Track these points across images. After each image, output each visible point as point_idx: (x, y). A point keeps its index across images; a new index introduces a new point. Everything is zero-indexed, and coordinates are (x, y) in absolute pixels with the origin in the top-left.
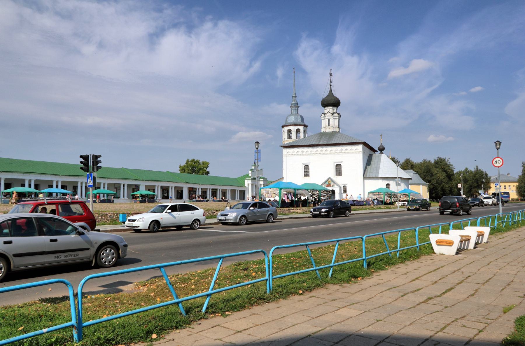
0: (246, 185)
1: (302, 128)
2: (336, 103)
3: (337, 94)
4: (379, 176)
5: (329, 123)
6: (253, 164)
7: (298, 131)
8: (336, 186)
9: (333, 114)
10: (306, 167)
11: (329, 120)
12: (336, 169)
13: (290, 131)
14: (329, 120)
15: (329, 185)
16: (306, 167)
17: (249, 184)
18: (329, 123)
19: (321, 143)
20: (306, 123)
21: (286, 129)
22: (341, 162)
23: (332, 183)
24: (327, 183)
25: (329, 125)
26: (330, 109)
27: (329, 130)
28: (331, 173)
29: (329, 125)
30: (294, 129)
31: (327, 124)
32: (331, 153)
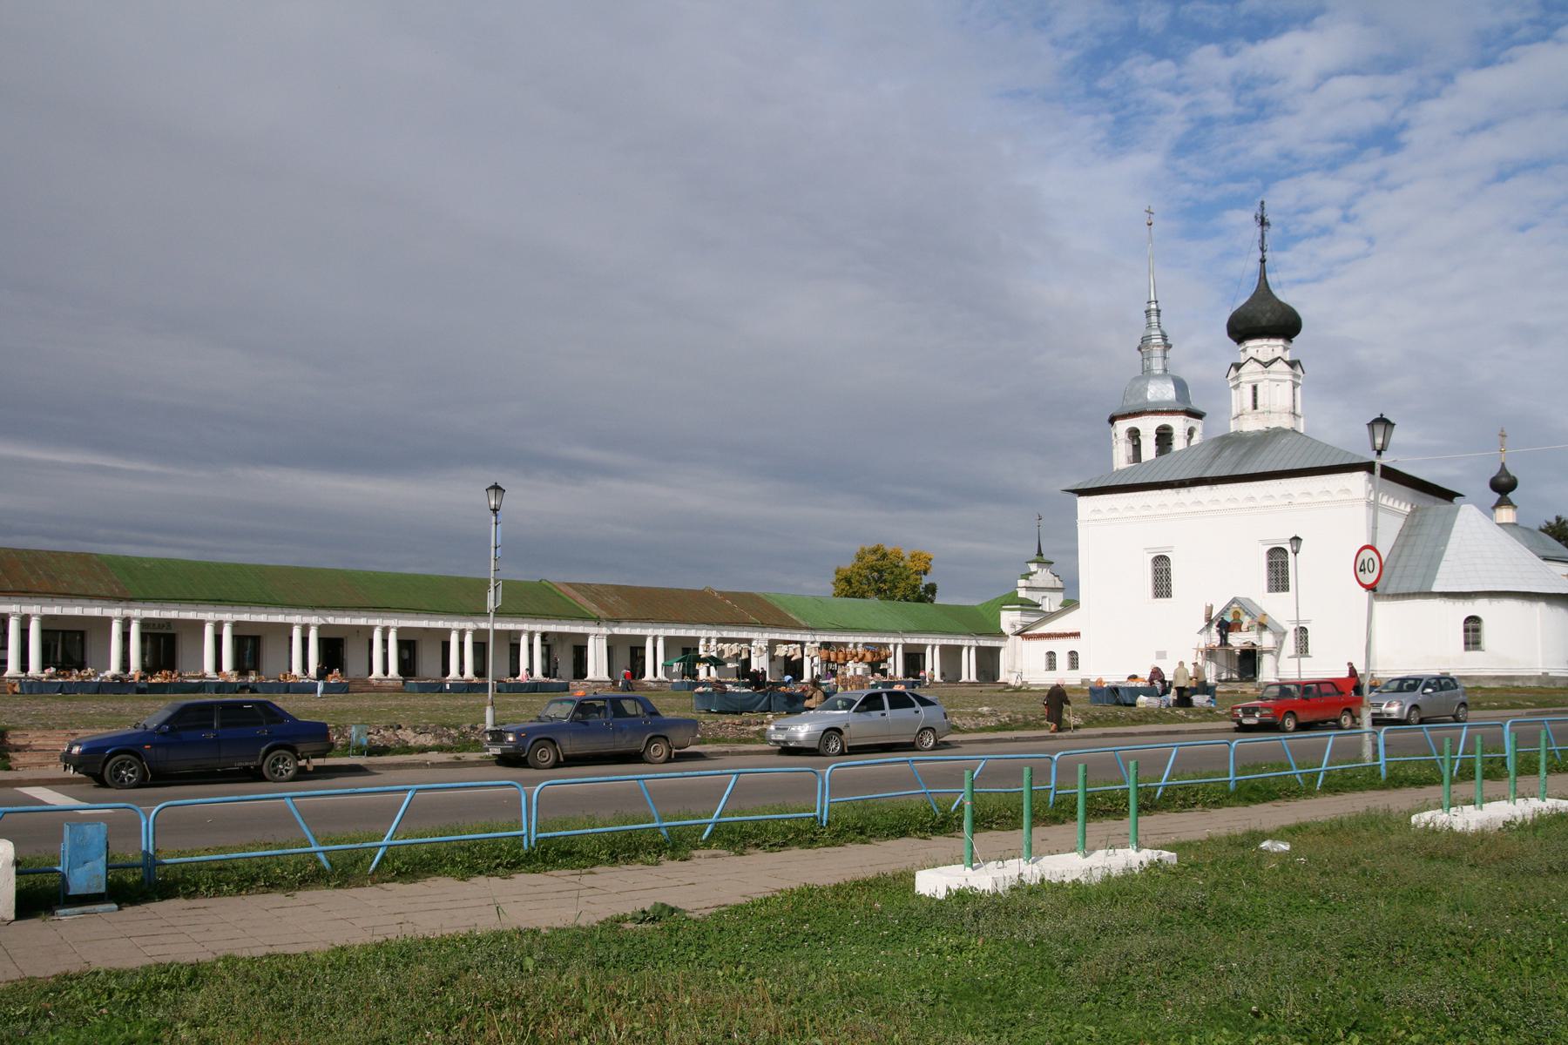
0: (1005, 627)
1: (1178, 424)
2: (1286, 326)
4: (1435, 589)
5: (1255, 401)
6: (1035, 557)
9: (1266, 365)
10: (1161, 566)
11: (1255, 388)
12: (1270, 565)
13: (1134, 434)
14: (1255, 388)
16: (1161, 566)
18: (1255, 401)
19: (1208, 474)
20: (1196, 405)
21: (1122, 426)
25: (1255, 407)
27: (1251, 425)
28: (1252, 585)
29: (1255, 407)
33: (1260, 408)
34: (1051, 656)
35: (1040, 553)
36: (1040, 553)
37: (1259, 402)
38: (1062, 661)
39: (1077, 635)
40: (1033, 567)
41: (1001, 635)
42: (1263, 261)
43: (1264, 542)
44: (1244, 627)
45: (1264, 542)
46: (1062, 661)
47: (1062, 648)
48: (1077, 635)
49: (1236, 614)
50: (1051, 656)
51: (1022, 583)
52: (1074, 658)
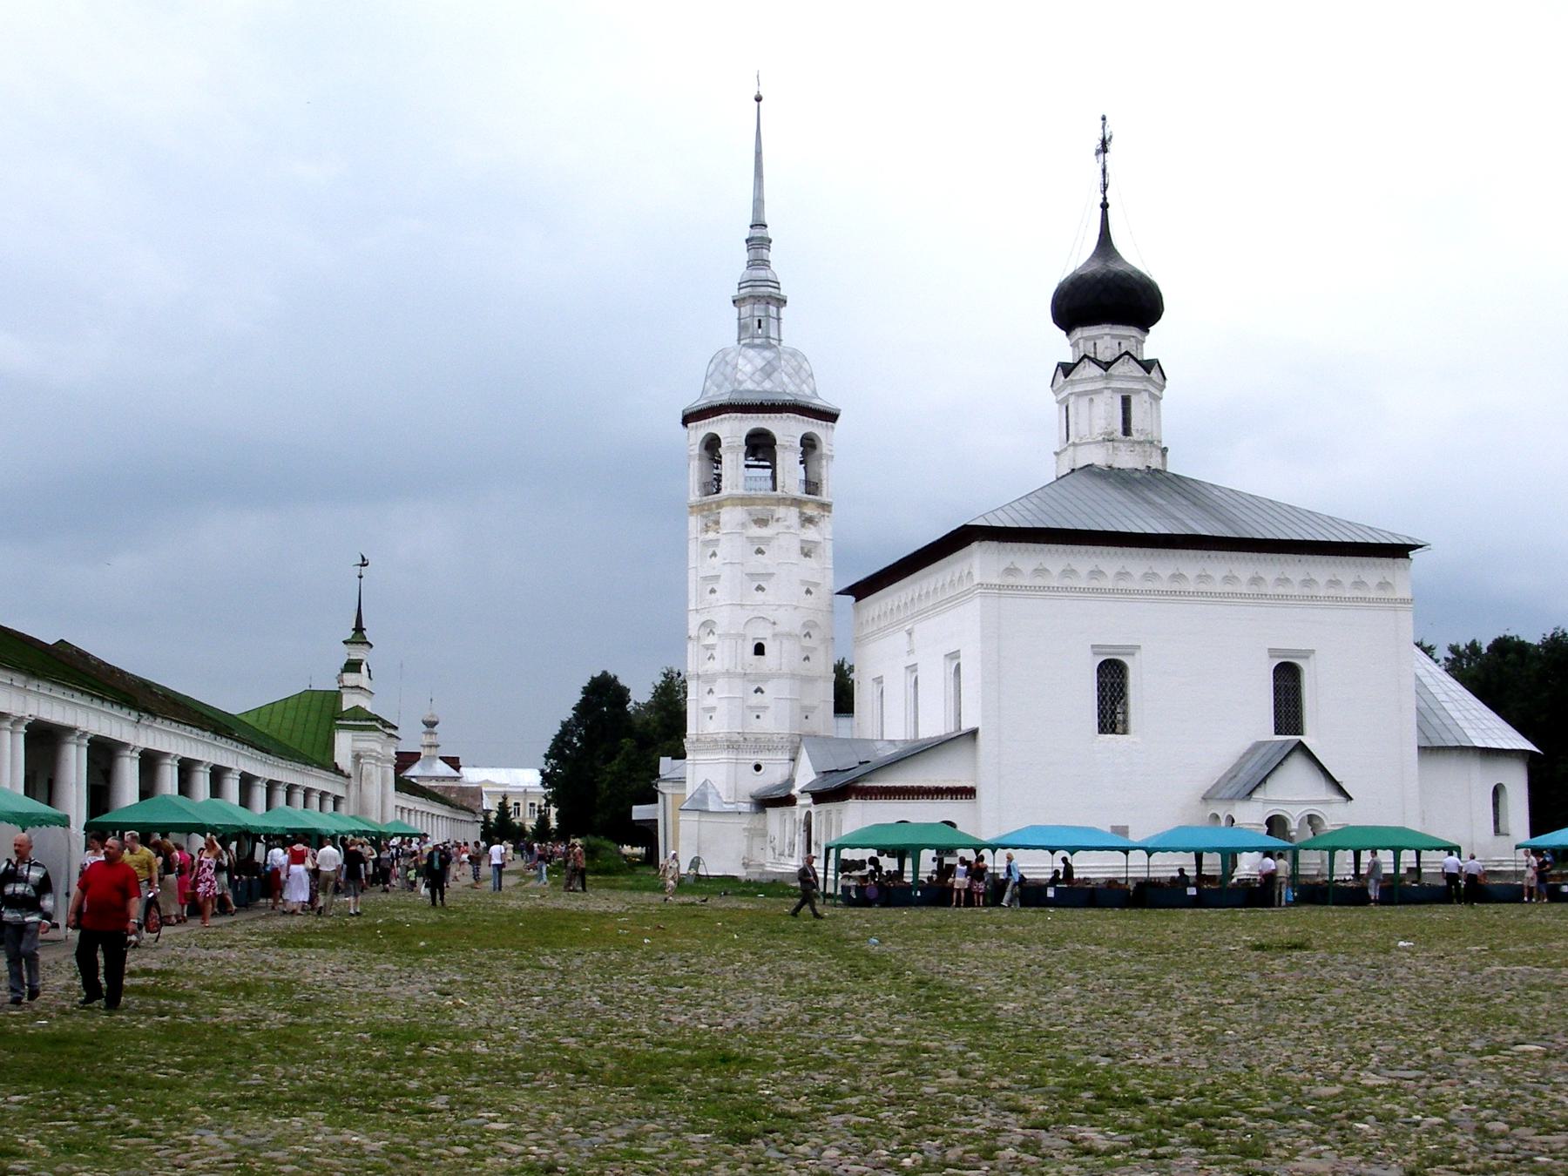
0: (343, 757)
3: (1138, 253)
6: (349, 635)
10: (1112, 679)
11: (1126, 402)
13: (760, 447)
14: (1126, 402)
16: (1112, 679)
17: (357, 757)
22: (1306, 654)
25: (1127, 431)
26: (1105, 338)
29: (1127, 431)
33: (1135, 436)
35: (359, 629)
36: (359, 629)
37: (1135, 423)
39: (968, 793)
40: (357, 653)
41: (337, 771)
42: (1105, 206)
43: (1273, 652)
45: (1273, 652)
48: (968, 793)
51: (350, 679)
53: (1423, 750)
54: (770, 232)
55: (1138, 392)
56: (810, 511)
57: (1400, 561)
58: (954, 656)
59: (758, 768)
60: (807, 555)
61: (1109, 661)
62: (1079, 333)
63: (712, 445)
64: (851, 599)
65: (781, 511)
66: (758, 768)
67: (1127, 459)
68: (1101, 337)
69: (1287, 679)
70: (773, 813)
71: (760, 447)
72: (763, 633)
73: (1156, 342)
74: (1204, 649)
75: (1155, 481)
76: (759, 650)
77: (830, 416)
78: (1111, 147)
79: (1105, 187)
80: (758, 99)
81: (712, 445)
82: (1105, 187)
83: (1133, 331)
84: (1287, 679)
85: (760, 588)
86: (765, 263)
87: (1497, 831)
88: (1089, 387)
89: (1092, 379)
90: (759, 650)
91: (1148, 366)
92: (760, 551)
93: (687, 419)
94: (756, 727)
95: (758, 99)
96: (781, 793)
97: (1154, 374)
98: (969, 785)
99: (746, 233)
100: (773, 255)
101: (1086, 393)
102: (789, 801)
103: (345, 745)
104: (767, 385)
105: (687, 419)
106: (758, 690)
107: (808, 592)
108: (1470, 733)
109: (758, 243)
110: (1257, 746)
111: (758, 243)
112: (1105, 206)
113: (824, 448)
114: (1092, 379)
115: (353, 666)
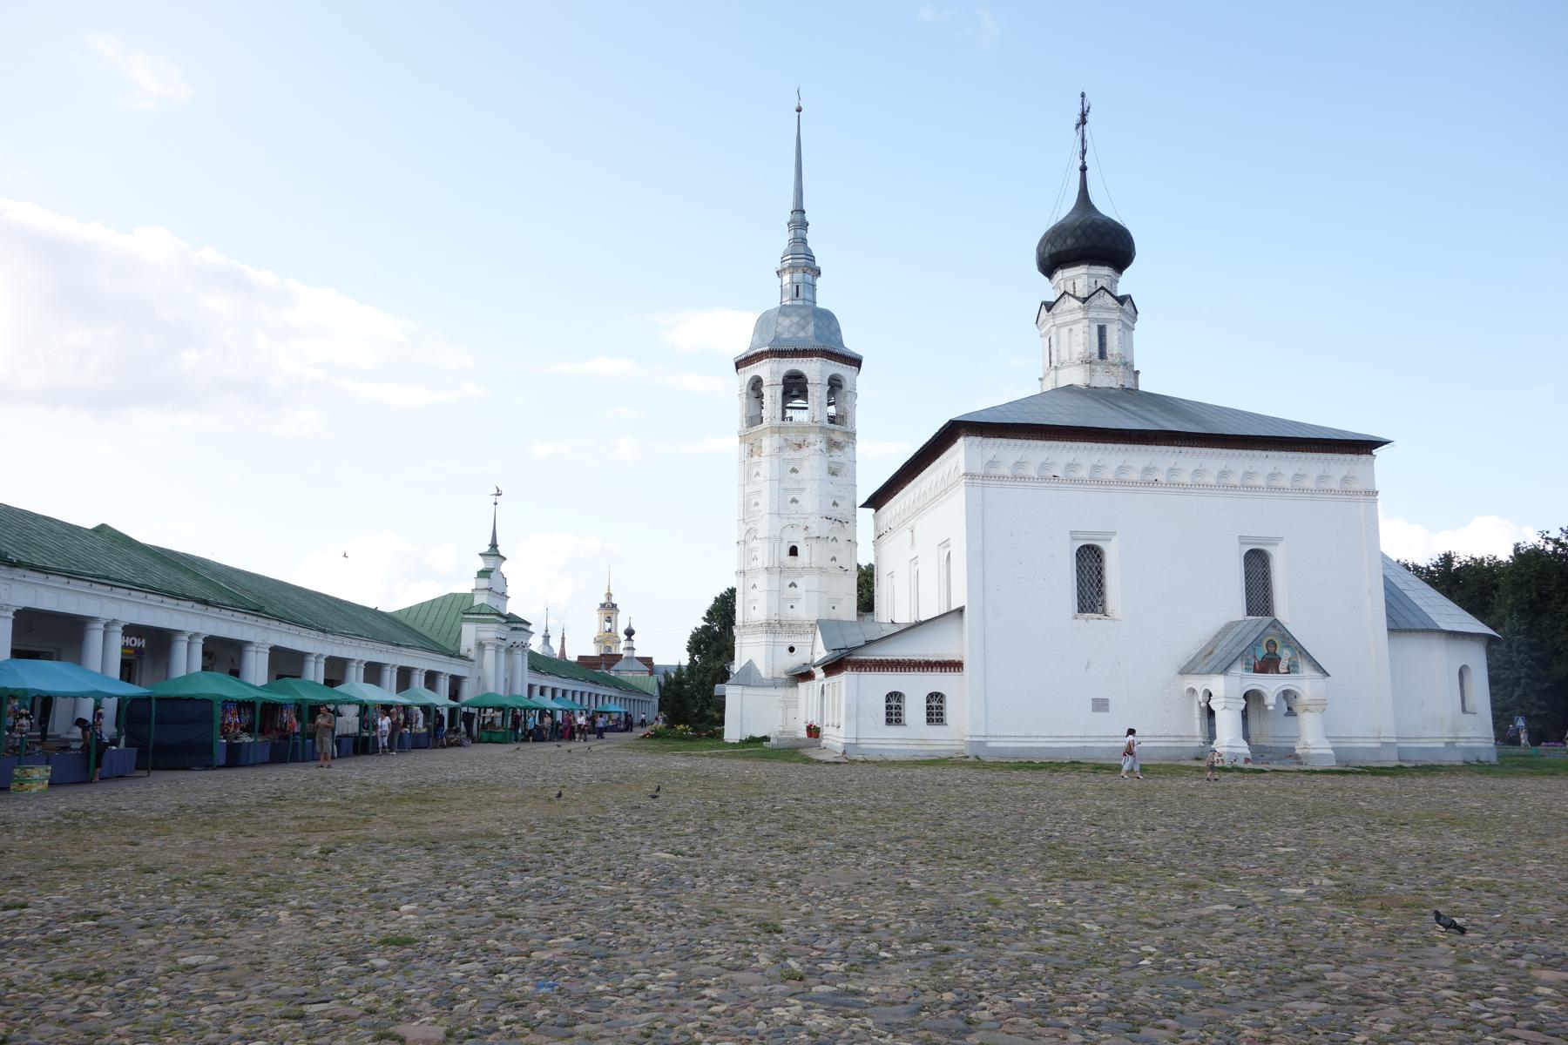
6: (486, 549)
7: (835, 385)
8: (1306, 670)
10: (1090, 560)
11: (1102, 331)
14: (1102, 331)
15: (1268, 665)
16: (1090, 560)
17: (481, 646)
22: (1275, 541)
23: (1285, 655)
24: (1262, 652)
25: (1102, 354)
29: (1102, 354)
30: (815, 371)
31: (1096, 350)
32: (1223, 485)
33: (1110, 359)
34: (894, 698)
35: (494, 545)
36: (494, 545)
38: (915, 709)
39: (956, 666)
41: (465, 658)
42: (1083, 169)
43: (1243, 540)
44: (1282, 667)
45: (1243, 540)
46: (915, 709)
47: (915, 688)
48: (956, 666)
49: (1271, 643)
50: (894, 698)
52: (935, 710)
53: (1390, 630)
54: (808, 217)
55: (1112, 321)
56: (837, 437)
57: (1364, 457)
58: (945, 543)
59: (792, 649)
60: (834, 474)
61: (1088, 546)
62: (1060, 275)
63: (756, 384)
64: (872, 511)
65: (812, 438)
66: (792, 649)
67: (1103, 380)
68: (1078, 276)
69: (1257, 564)
70: (802, 686)
71: (795, 387)
72: (798, 539)
73: (1127, 283)
74: (1177, 534)
75: (1131, 395)
76: (794, 551)
77: (856, 362)
78: (1089, 118)
79: (1084, 152)
80: (799, 110)
81: (756, 384)
82: (1084, 152)
83: (1106, 271)
84: (1257, 564)
85: (794, 501)
86: (804, 241)
87: (1464, 711)
88: (1068, 318)
89: (1071, 311)
90: (794, 551)
91: (1122, 300)
92: (794, 471)
93: (740, 364)
94: (790, 615)
95: (799, 110)
96: (804, 670)
97: (1126, 306)
98: (957, 659)
99: (788, 217)
100: (811, 236)
101: (1065, 324)
102: (807, 676)
103: (470, 635)
104: (801, 334)
105: (740, 364)
106: (793, 585)
107: (835, 504)
108: (1435, 618)
109: (799, 222)
110: (1230, 626)
111: (799, 222)
112: (1083, 169)
113: (847, 386)
114: (1071, 311)
115: (484, 574)
